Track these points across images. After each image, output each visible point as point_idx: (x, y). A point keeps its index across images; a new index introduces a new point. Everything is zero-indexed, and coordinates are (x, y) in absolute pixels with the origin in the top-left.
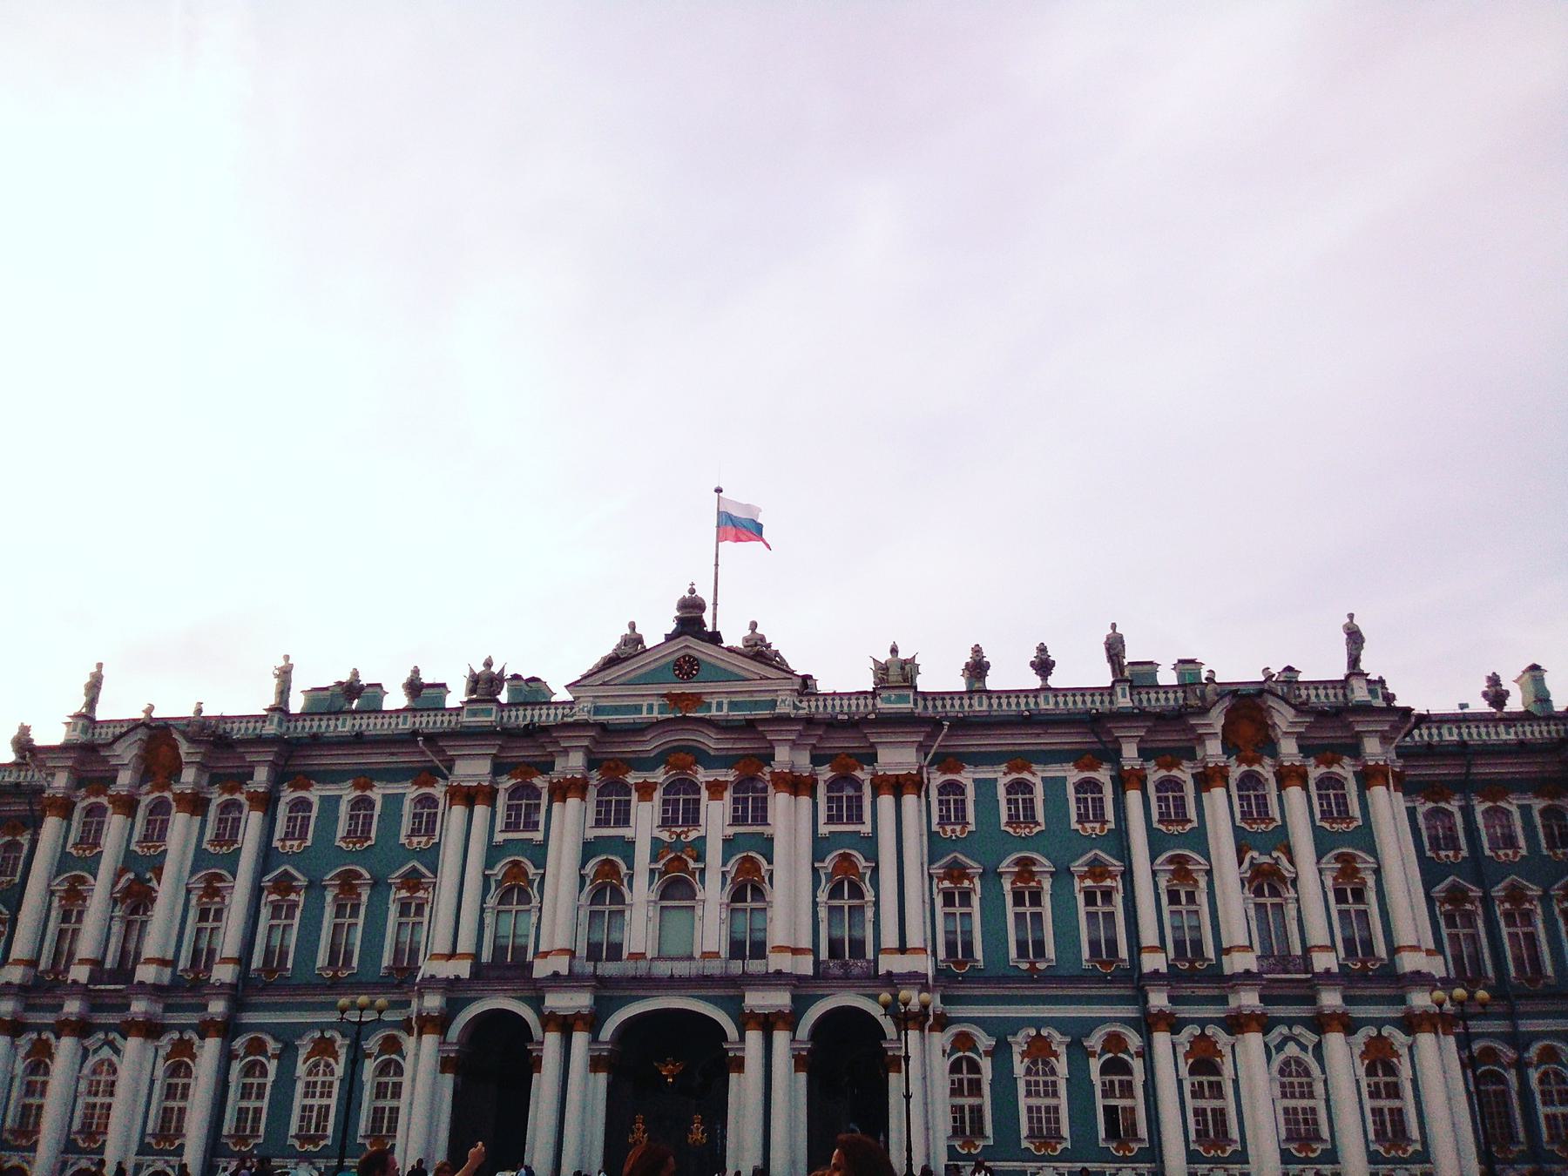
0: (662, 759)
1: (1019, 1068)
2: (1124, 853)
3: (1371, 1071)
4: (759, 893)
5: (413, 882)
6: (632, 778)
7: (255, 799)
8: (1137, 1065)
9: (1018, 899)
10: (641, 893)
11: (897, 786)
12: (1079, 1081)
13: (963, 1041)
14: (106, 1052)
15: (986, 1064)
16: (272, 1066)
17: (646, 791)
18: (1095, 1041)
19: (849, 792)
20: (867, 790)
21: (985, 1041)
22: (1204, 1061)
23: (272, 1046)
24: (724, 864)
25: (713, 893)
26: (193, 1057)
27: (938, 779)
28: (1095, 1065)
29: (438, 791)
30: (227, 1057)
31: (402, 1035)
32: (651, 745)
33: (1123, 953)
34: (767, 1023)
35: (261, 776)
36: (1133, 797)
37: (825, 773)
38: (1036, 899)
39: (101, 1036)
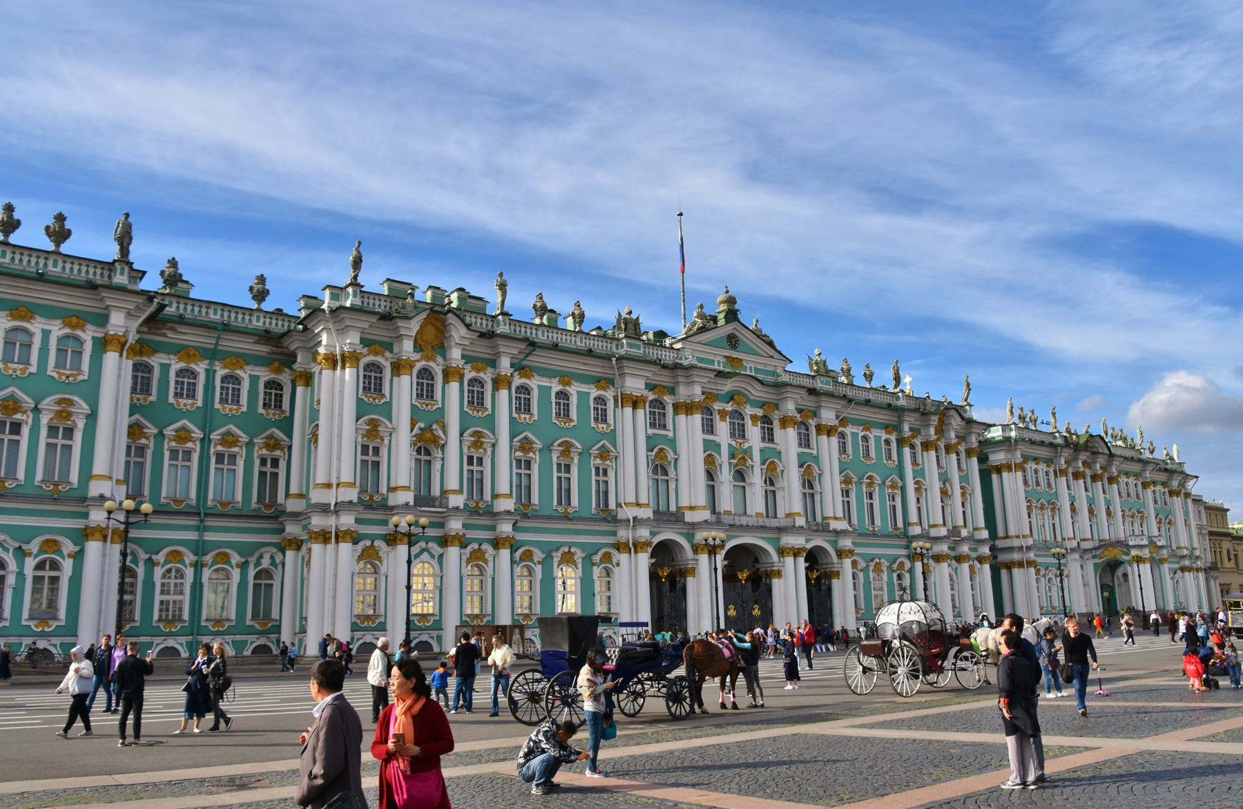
0: (731, 397)
4: (772, 484)
6: (717, 406)
8: (908, 575)
10: (725, 476)
12: (890, 583)
15: (861, 575)
17: (723, 413)
19: (803, 431)
20: (813, 431)
23: (538, 555)
24: (763, 464)
25: (756, 479)
26: (486, 561)
28: (895, 575)
29: (609, 395)
30: (513, 562)
31: (614, 552)
33: (900, 524)
34: (796, 553)
35: (505, 364)
39: (423, 544)
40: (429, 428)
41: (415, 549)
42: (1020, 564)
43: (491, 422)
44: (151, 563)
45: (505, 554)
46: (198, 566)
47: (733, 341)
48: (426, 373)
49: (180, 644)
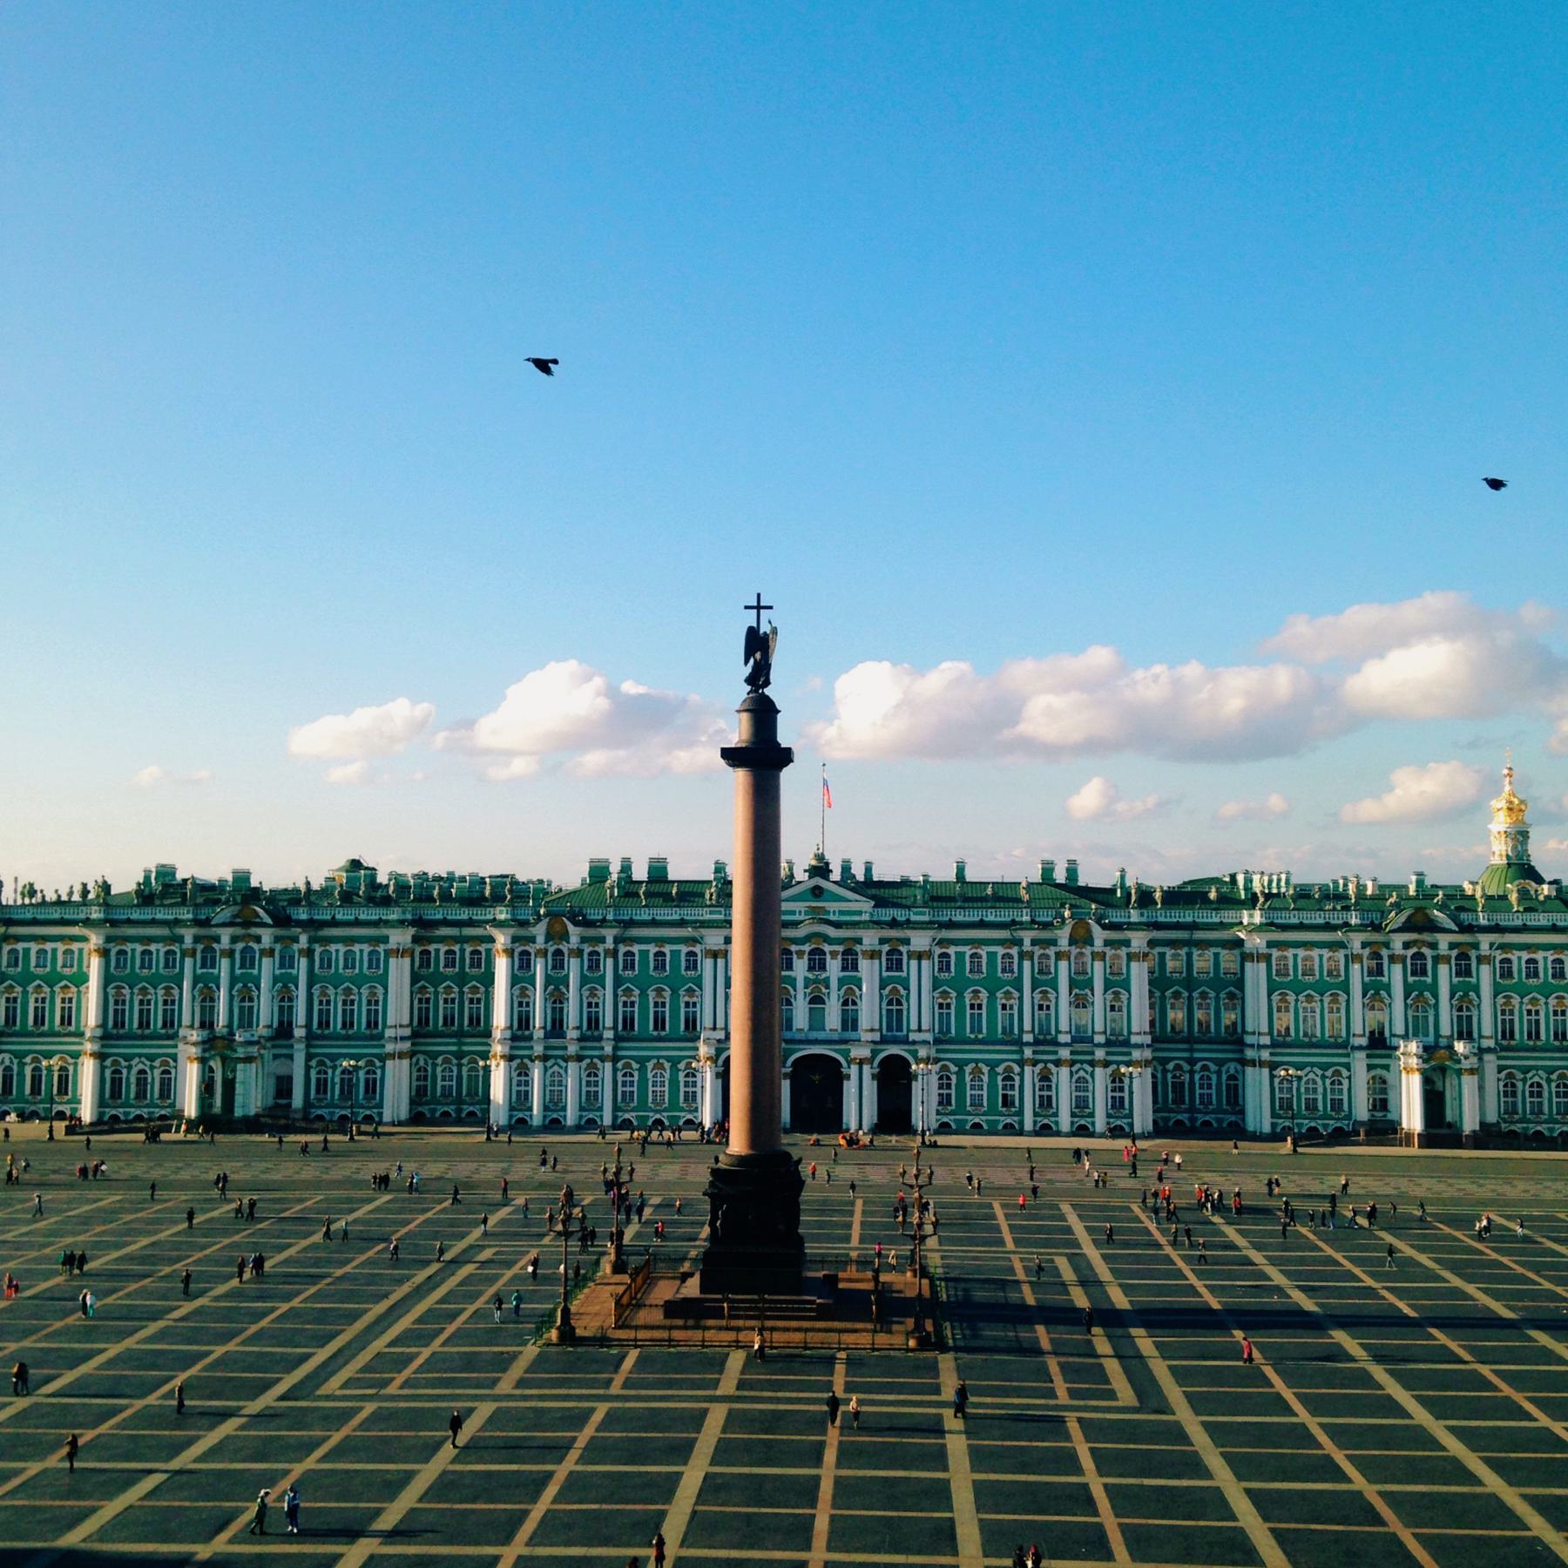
1: (968, 1079)
2: (1020, 990)
3: (1113, 1081)
5: (690, 992)
6: (793, 948)
7: (607, 952)
8: (1017, 1078)
9: (972, 1007)
11: (920, 956)
13: (945, 1068)
14: (556, 1068)
15: (954, 1077)
16: (636, 1074)
17: (800, 954)
18: (1000, 1069)
21: (954, 1068)
22: (1045, 1077)
27: (938, 951)
28: (1000, 1078)
29: (697, 949)
30: (615, 1070)
32: (800, 932)
34: (861, 1063)
36: (1027, 964)
37: (886, 948)
38: (980, 1007)
40: (557, 989)
41: (549, 1064)
42: (1253, 1063)
43: (601, 981)
44: (435, 1065)
45: (608, 1066)
46: (460, 1066)
47: (817, 892)
48: (558, 953)
49: (451, 1109)
